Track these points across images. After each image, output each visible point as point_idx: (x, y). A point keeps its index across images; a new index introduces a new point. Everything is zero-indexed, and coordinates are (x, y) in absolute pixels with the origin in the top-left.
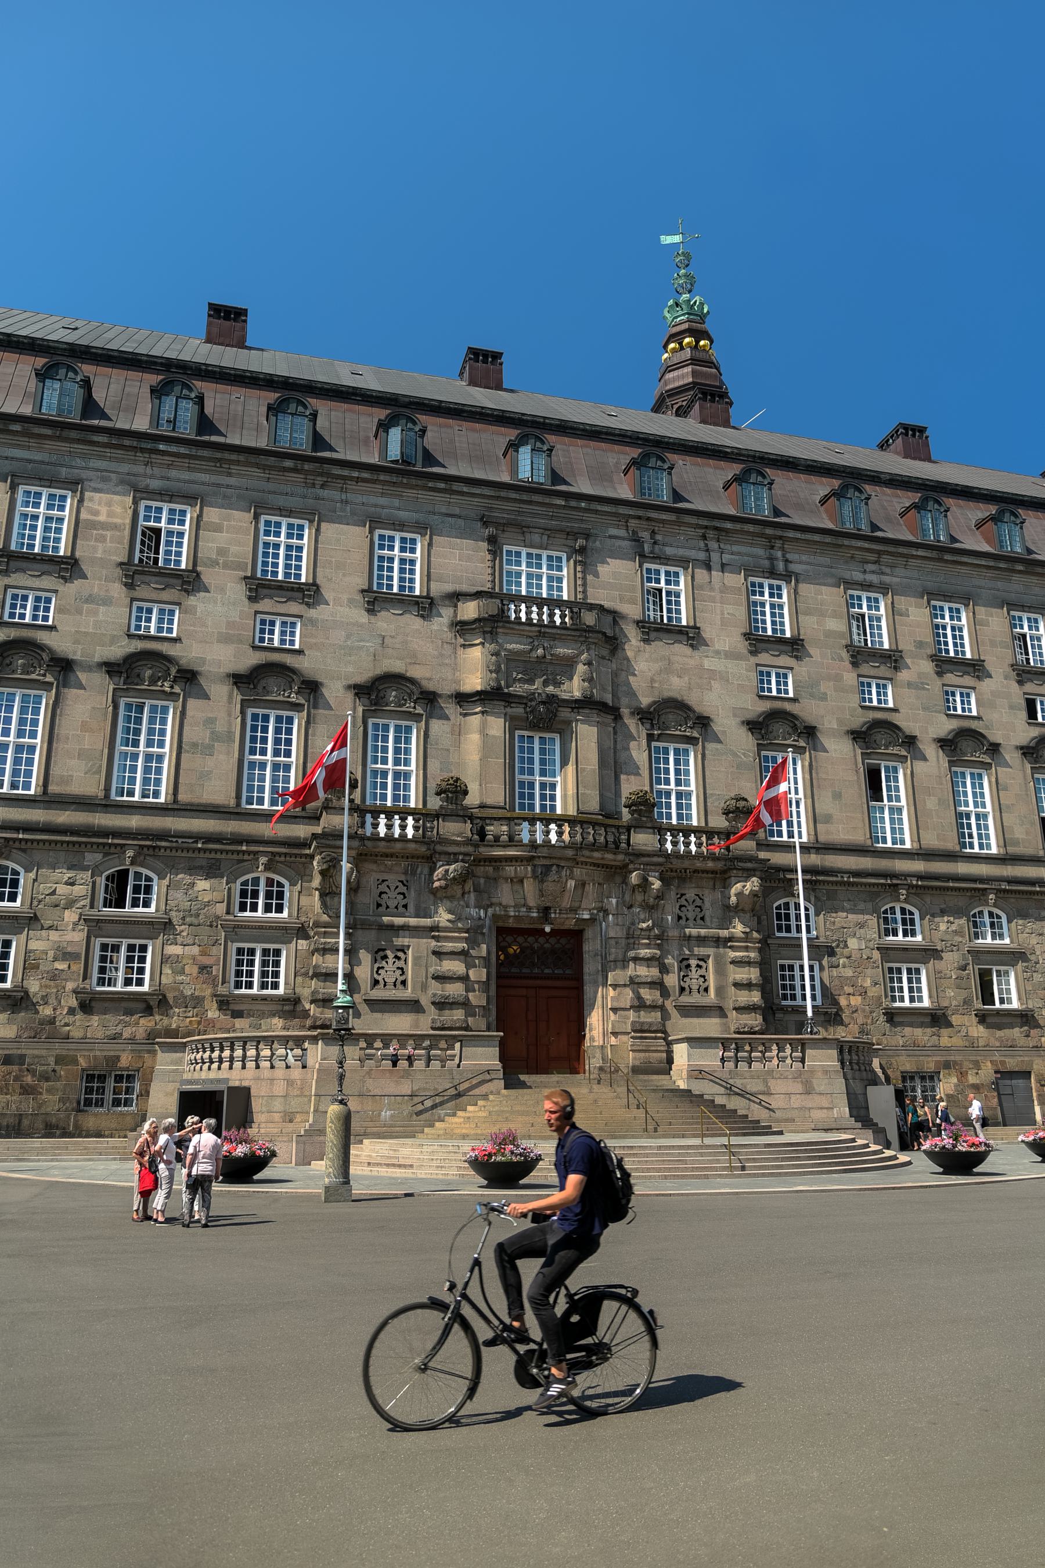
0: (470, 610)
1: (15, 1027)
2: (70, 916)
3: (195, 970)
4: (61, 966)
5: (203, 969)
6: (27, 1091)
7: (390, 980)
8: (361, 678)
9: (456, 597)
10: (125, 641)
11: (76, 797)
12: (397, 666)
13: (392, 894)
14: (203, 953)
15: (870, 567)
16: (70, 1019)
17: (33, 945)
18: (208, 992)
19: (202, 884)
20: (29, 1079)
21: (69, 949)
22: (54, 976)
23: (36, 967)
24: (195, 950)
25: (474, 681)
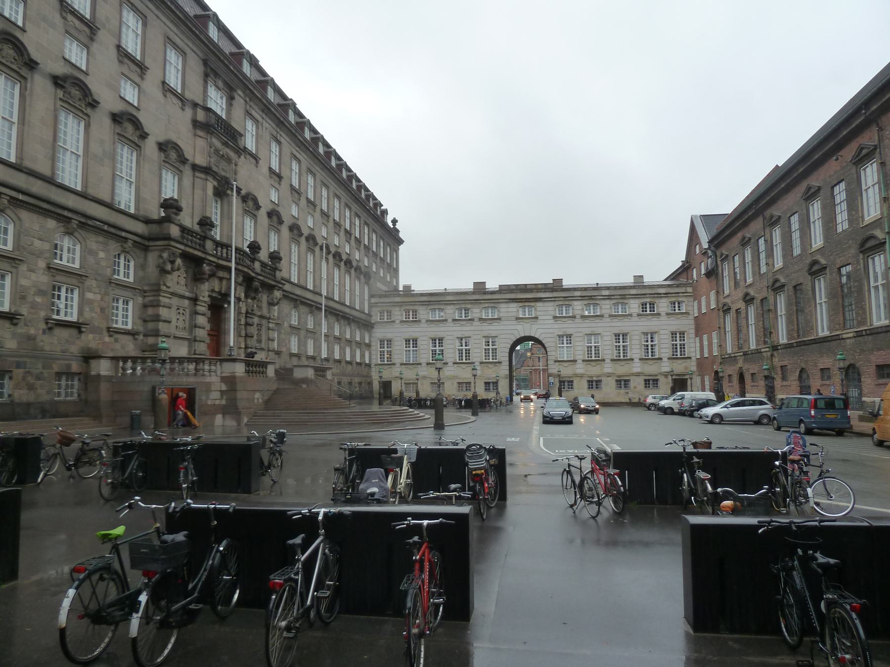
0: (201, 116)
1: (15, 342)
2: (42, 264)
3: (98, 310)
4: (39, 299)
5: (102, 310)
6: (31, 387)
7: (181, 326)
8: (161, 139)
9: (195, 105)
10: (62, 63)
11: (40, 174)
12: (174, 138)
13: (182, 277)
14: (102, 300)
15: (297, 148)
16: (44, 337)
17: (24, 282)
18: (104, 326)
19: (102, 255)
20: (30, 379)
21: (41, 288)
22: (34, 306)
23: (23, 298)
24: (99, 297)
25: (200, 161)
